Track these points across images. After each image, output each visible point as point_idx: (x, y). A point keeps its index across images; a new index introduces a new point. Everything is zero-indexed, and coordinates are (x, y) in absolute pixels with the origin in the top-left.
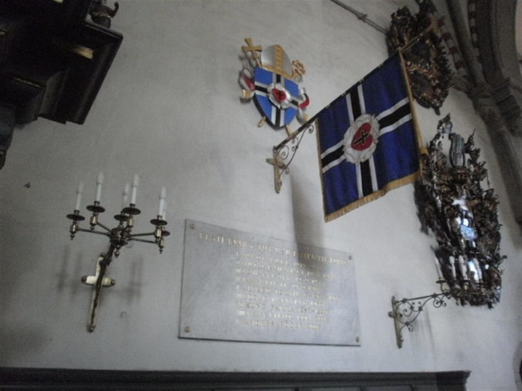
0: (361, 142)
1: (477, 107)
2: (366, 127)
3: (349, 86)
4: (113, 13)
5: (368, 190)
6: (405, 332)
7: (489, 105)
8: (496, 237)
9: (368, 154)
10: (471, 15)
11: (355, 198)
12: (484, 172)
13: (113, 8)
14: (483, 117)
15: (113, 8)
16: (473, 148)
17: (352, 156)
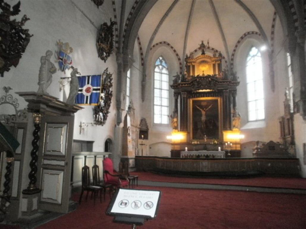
0: (88, 90)
1: (117, 60)
2: (89, 88)
3: (88, 75)
4: (31, 36)
5: (87, 103)
6: (82, 131)
7: (121, 61)
8: (109, 106)
9: (89, 95)
10: (126, 25)
11: (83, 103)
12: (112, 85)
13: (31, 35)
14: (118, 63)
15: (31, 35)
16: (111, 78)
17: (84, 92)
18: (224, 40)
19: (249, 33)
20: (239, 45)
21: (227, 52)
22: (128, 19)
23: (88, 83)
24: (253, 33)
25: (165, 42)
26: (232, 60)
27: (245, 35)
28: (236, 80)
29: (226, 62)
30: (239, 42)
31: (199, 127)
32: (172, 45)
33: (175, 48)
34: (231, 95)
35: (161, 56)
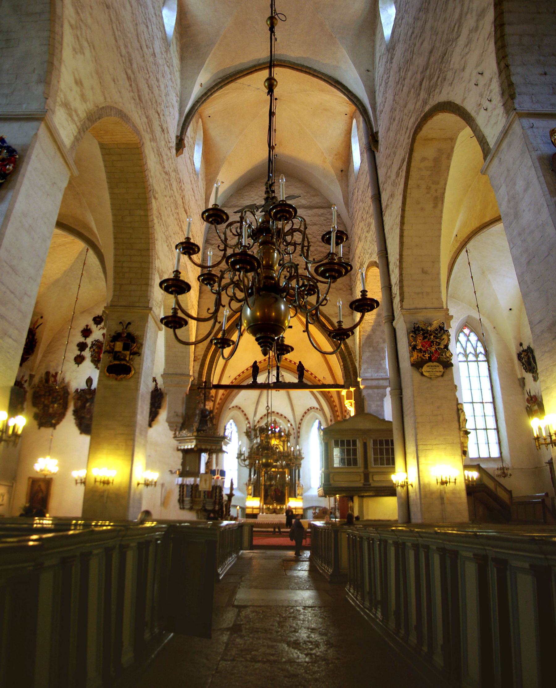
18: (293, 410)
19: (314, 408)
20: (305, 416)
21: (295, 421)
22: (219, 404)
23: (218, 474)
24: (317, 409)
25: (236, 406)
26: (299, 428)
27: (311, 408)
28: (301, 455)
29: (293, 429)
30: (305, 413)
31: (269, 493)
32: (243, 409)
33: (246, 411)
34: (297, 468)
35: (232, 419)
